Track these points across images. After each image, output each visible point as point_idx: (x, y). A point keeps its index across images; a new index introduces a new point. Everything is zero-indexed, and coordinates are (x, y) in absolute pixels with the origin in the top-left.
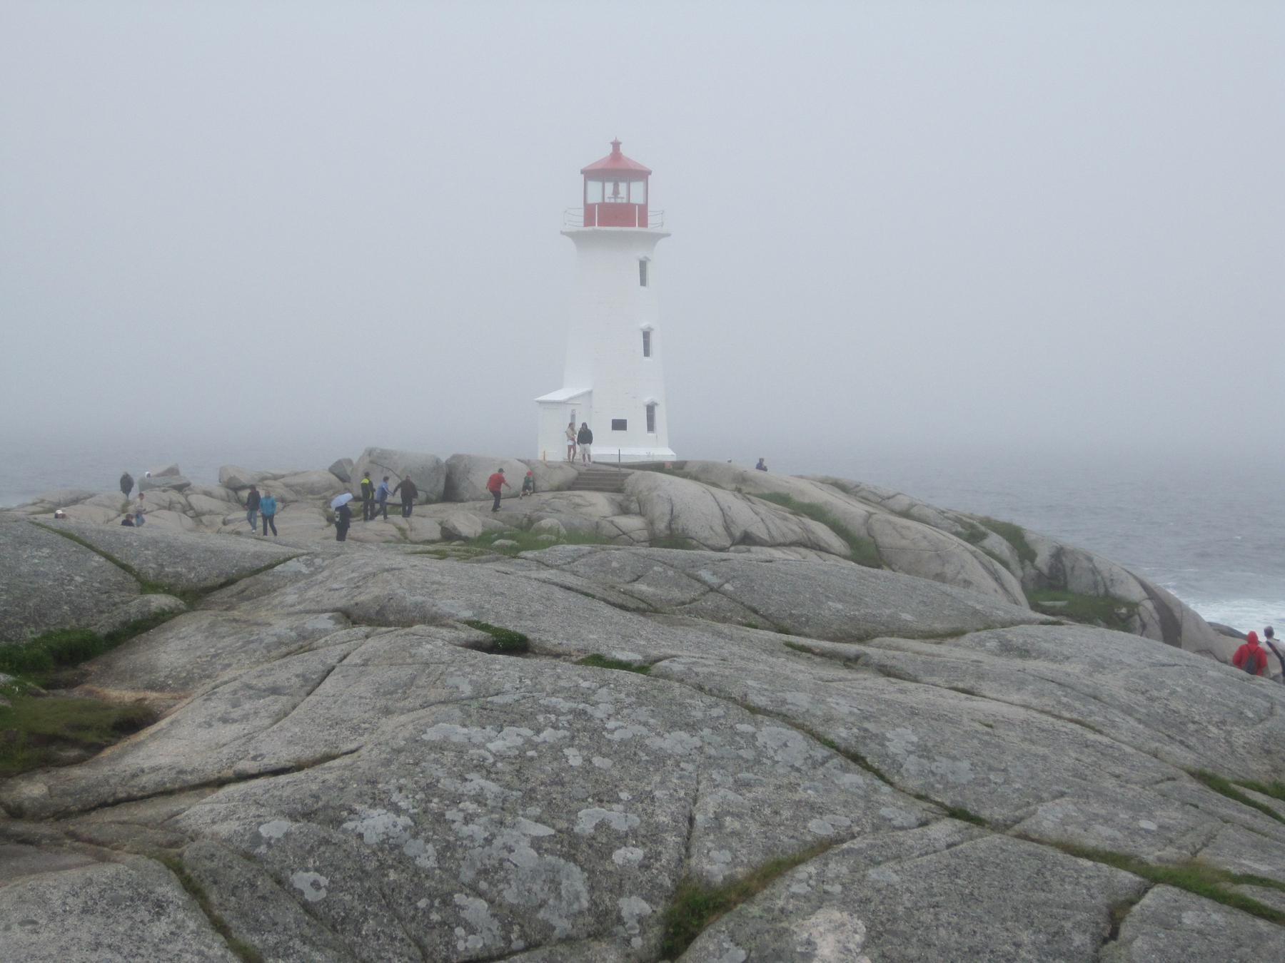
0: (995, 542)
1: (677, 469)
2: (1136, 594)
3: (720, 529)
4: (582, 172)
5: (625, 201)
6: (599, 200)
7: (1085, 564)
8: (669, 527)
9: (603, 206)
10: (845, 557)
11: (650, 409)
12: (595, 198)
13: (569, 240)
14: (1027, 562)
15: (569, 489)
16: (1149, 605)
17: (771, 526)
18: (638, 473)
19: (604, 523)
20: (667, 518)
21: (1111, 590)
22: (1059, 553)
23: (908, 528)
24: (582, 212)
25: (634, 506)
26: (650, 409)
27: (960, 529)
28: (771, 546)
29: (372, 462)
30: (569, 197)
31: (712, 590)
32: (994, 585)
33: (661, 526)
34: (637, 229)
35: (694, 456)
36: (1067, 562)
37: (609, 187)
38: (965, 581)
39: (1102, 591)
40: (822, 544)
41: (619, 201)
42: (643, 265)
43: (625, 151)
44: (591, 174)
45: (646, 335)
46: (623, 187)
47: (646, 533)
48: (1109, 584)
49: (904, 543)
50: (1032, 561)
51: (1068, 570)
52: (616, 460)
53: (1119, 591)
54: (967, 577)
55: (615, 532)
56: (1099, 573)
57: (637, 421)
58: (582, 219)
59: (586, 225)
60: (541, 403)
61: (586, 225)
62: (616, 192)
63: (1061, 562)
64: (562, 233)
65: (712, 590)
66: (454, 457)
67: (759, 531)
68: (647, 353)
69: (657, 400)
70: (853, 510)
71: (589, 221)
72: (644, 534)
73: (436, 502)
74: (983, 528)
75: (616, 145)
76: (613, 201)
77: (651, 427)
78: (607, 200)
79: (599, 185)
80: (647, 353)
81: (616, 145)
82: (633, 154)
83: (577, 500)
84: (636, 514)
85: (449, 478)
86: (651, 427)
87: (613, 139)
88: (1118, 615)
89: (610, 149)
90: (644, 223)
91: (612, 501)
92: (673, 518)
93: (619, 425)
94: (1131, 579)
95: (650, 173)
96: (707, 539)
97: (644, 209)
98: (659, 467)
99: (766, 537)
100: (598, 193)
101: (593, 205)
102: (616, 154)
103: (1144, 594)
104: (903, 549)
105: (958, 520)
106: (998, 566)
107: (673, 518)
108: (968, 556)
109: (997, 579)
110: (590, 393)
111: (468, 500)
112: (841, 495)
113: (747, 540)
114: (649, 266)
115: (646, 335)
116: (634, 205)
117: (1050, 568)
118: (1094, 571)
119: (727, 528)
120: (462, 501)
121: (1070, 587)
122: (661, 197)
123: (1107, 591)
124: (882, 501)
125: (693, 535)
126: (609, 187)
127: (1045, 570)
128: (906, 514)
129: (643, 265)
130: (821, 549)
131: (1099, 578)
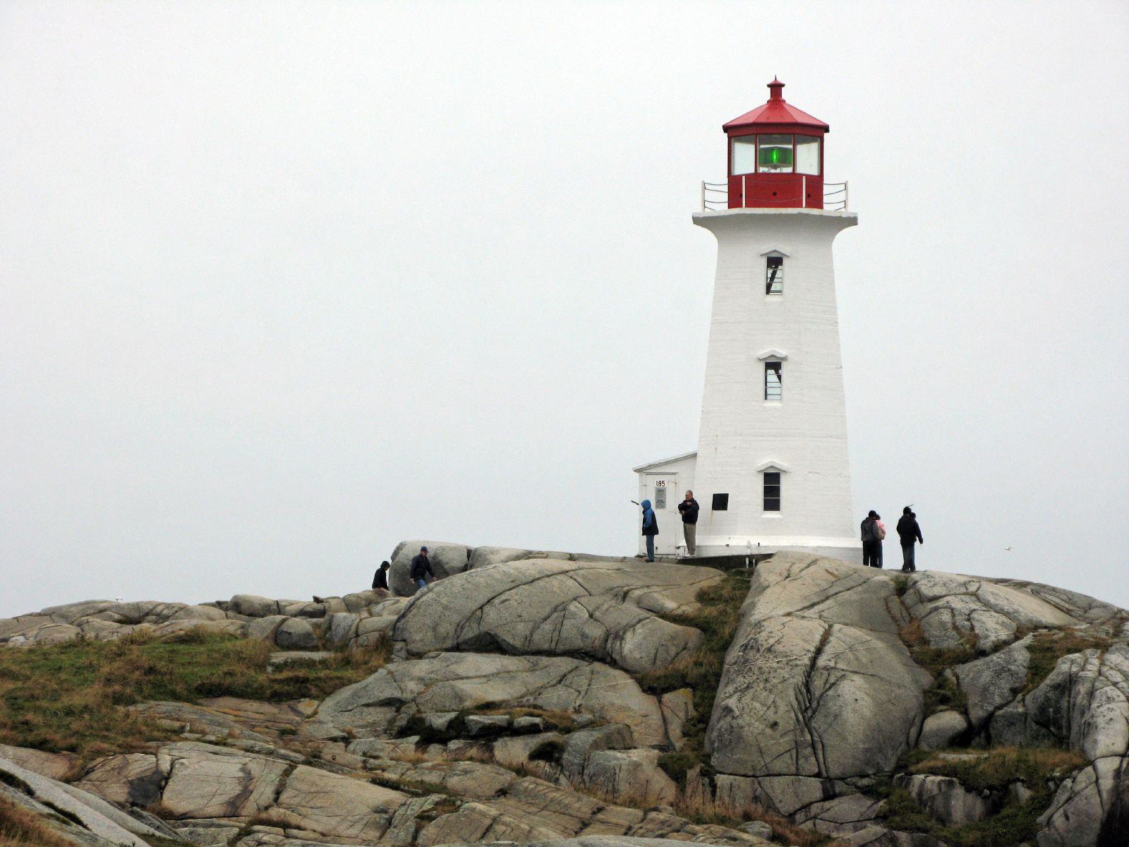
3: (446, 628)
11: (772, 482)
26: (772, 482)
43: (786, 94)
44: (735, 132)
57: (749, 493)
60: (639, 471)
64: (698, 221)
75: (776, 88)
81: (776, 88)
87: (771, 81)
89: (766, 95)
90: (816, 198)
95: (826, 129)
99: (518, 643)
110: (694, 456)
116: (801, 175)
117: (1043, 709)
119: (460, 627)
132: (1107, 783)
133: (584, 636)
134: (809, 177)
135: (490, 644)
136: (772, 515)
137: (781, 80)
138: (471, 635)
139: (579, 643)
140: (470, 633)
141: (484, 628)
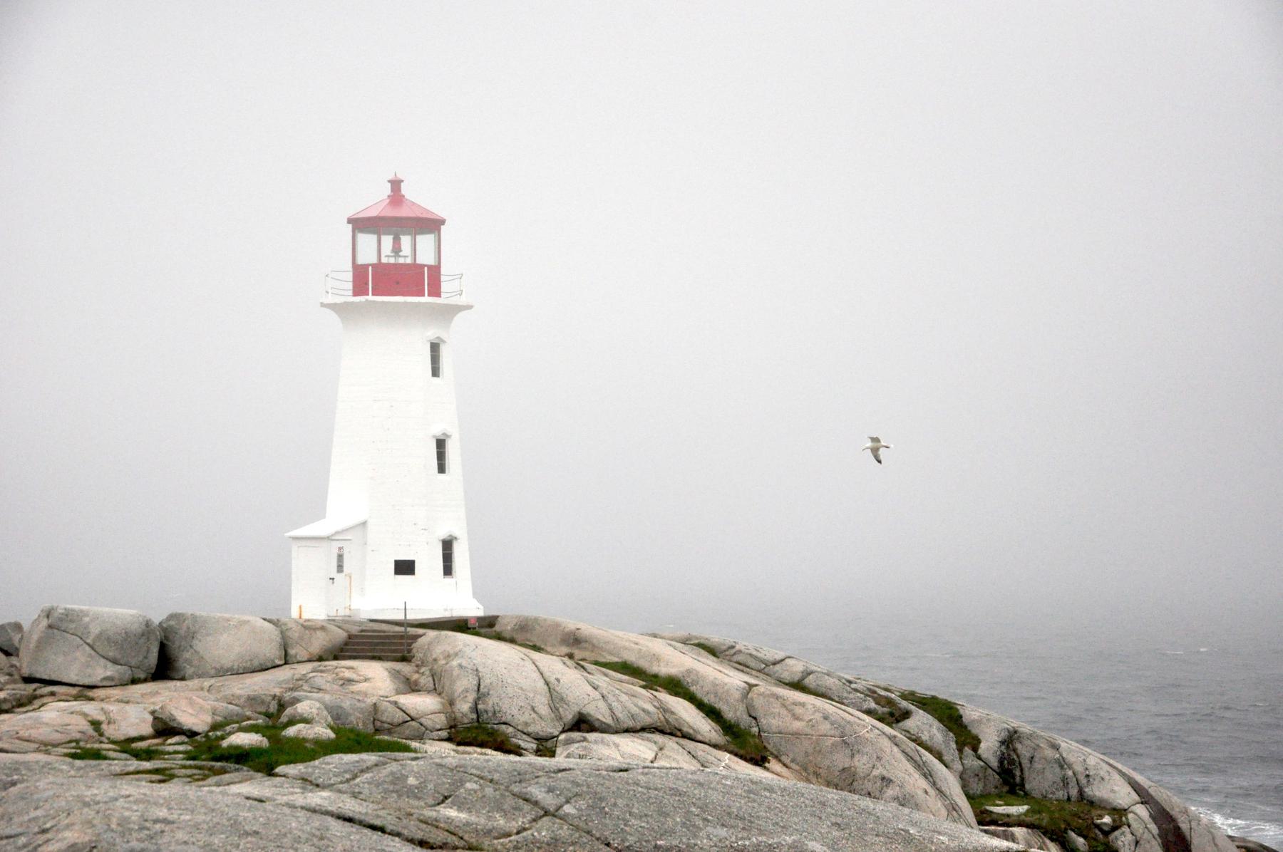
0: (921, 722)
1: (486, 627)
2: (1122, 795)
3: (544, 710)
4: (350, 221)
5: (409, 261)
6: (375, 261)
7: (1050, 753)
8: (475, 709)
9: (379, 268)
10: (715, 746)
11: (447, 545)
12: (367, 255)
13: (333, 317)
14: (967, 750)
15: (336, 658)
16: (1142, 811)
17: (615, 704)
18: (432, 634)
19: (384, 705)
20: (471, 697)
21: (1088, 791)
22: (1010, 739)
23: (803, 705)
24: (349, 276)
25: (425, 680)
26: (447, 545)
27: (873, 705)
28: (617, 732)
29: (50, 627)
30: (334, 256)
31: (546, 813)
32: (923, 783)
33: (464, 707)
34: (426, 299)
35: (510, 610)
36: (1023, 750)
37: (387, 241)
38: (883, 778)
39: (1074, 792)
40: (685, 729)
41: (401, 261)
42: (435, 348)
43: (405, 190)
45: (441, 444)
46: (406, 241)
47: (443, 717)
48: (1083, 781)
49: (797, 725)
50: (975, 749)
51: (1025, 762)
52: (399, 616)
53: (1097, 791)
54: (885, 773)
55: (400, 717)
56: (1070, 767)
57: (428, 562)
58: (350, 286)
59: (356, 294)
61: (356, 294)
62: (397, 249)
63: (1015, 750)
65: (546, 813)
66: (172, 617)
67: (598, 712)
68: (442, 469)
69: (456, 533)
70: (723, 680)
71: (359, 289)
72: (441, 720)
73: (145, 681)
74: (905, 704)
75: (396, 184)
76: (392, 260)
77: (448, 570)
78: (384, 260)
79: (374, 238)
80: (442, 469)
81: (396, 184)
82: (421, 197)
83: (348, 674)
84: (429, 692)
85: (163, 648)
86: (448, 570)
87: (391, 177)
88: (1098, 827)
89: (387, 190)
90: (435, 291)
91: (395, 675)
92: (480, 695)
93: (404, 568)
94: (1117, 777)
96: (526, 724)
97: (435, 271)
98: (461, 625)
99: (609, 721)
100: (370, 249)
101: (366, 266)
102: (396, 195)
103: (1137, 798)
104: (797, 734)
105: (871, 693)
106: (928, 756)
107: (480, 695)
108: (886, 743)
109: (928, 775)
110: (364, 524)
111: (191, 678)
112: (710, 660)
113: (582, 724)
114: (445, 352)
115: (441, 444)
116: (422, 266)
117: (1001, 762)
118: (1062, 764)
119: (554, 709)
120: (183, 679)
121: (1027, 787)
122: (458, 256)
123: (1081, 792)
124: (765, 668)
125: (508, 718)
126: (387, 241)
127: (994, 763)
128: (798, 686)
129: (435, 348)
130: (685, 736)
131: (1070, 773)
132: (1154, 828)
133: (644, 710)
134: (430, 267)
135: (582, 724)
136: (448, 580)
137: (400, 177)
138: (570, 717)
139: (647, 720)
140: (569, 716)
141: (576, 709)
